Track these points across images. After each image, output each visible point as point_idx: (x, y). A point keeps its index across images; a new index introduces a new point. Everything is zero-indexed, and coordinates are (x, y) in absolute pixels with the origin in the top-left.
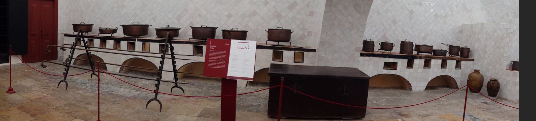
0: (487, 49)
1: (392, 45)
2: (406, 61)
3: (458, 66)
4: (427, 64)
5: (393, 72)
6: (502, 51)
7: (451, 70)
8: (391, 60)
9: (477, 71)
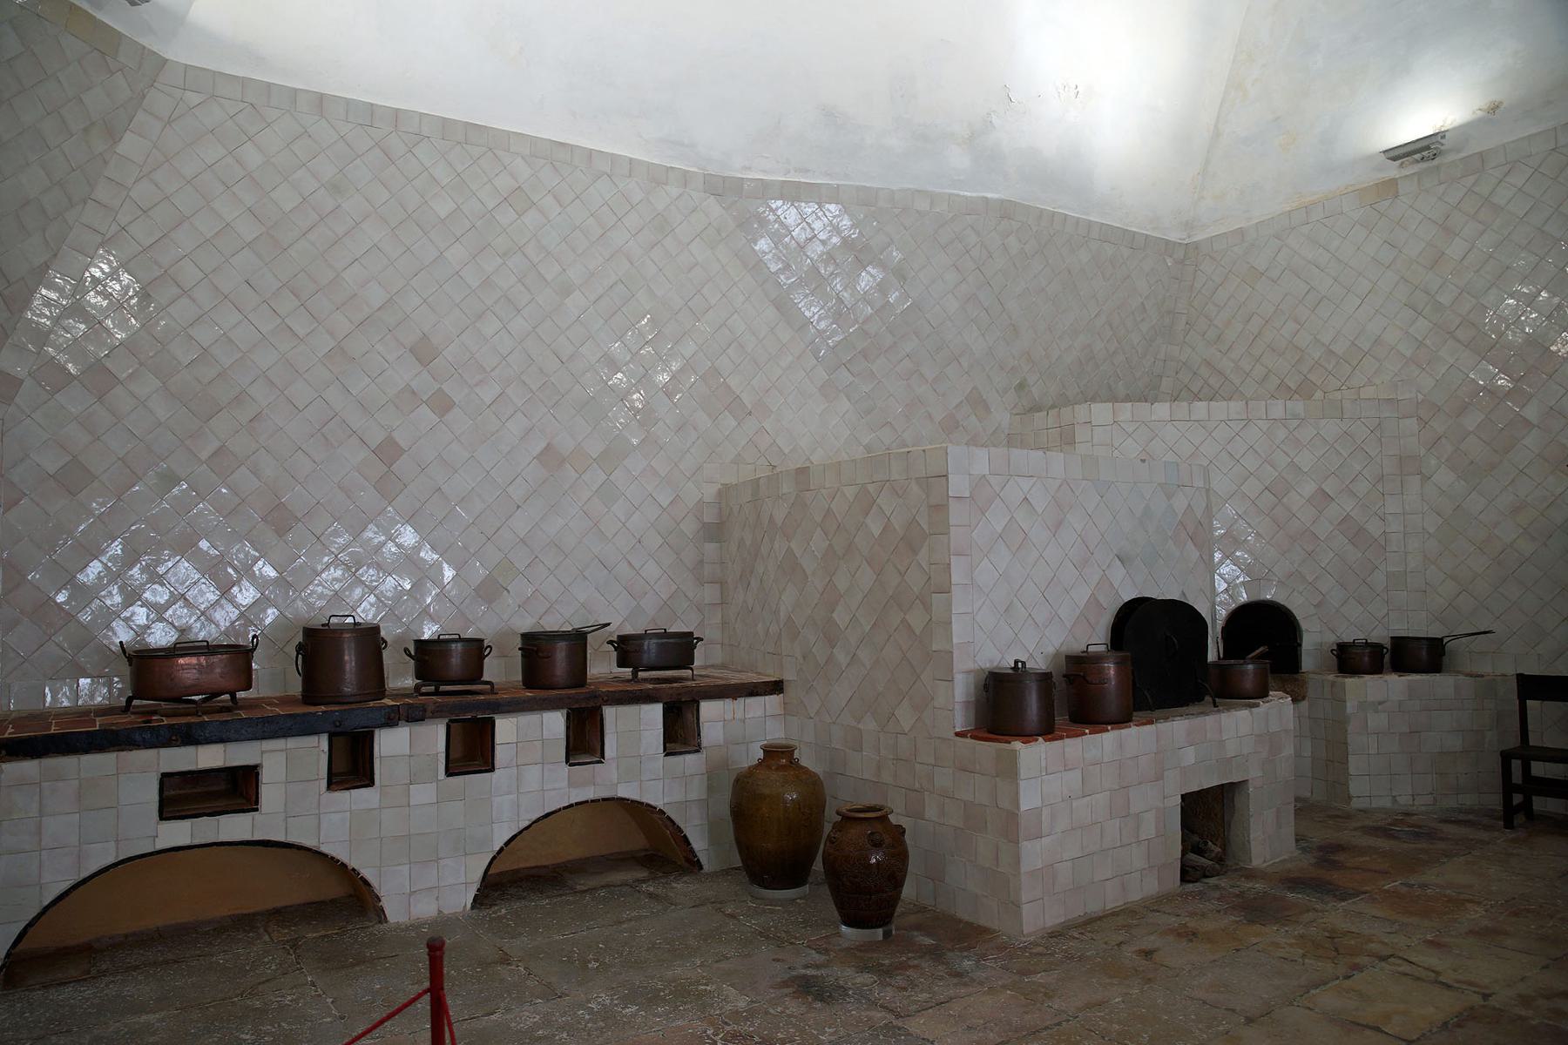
0: (841, 617)
6: (917, 619)
8: (210, 757)
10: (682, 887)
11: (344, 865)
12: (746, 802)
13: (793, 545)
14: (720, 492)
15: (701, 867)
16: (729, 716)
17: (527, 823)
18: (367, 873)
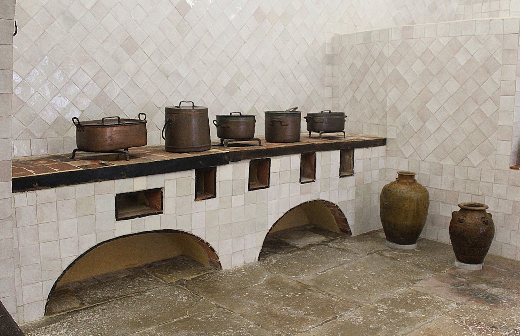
0: (432, 106)
1: (139, 126)
2: (189, 178)
3: (346, 168)
4: (259, 178)
5: (151, 223)
6: (488, 109)
7: (329, 184)
9: (406, 178)
10: (348, 244)
11: (203, 241)
12: (389, 202)
13: (398, 68)
14: (333, 39)
15: (351, 234)
16: (365, 157)
17: (283, 214)
18: (213, 245)
